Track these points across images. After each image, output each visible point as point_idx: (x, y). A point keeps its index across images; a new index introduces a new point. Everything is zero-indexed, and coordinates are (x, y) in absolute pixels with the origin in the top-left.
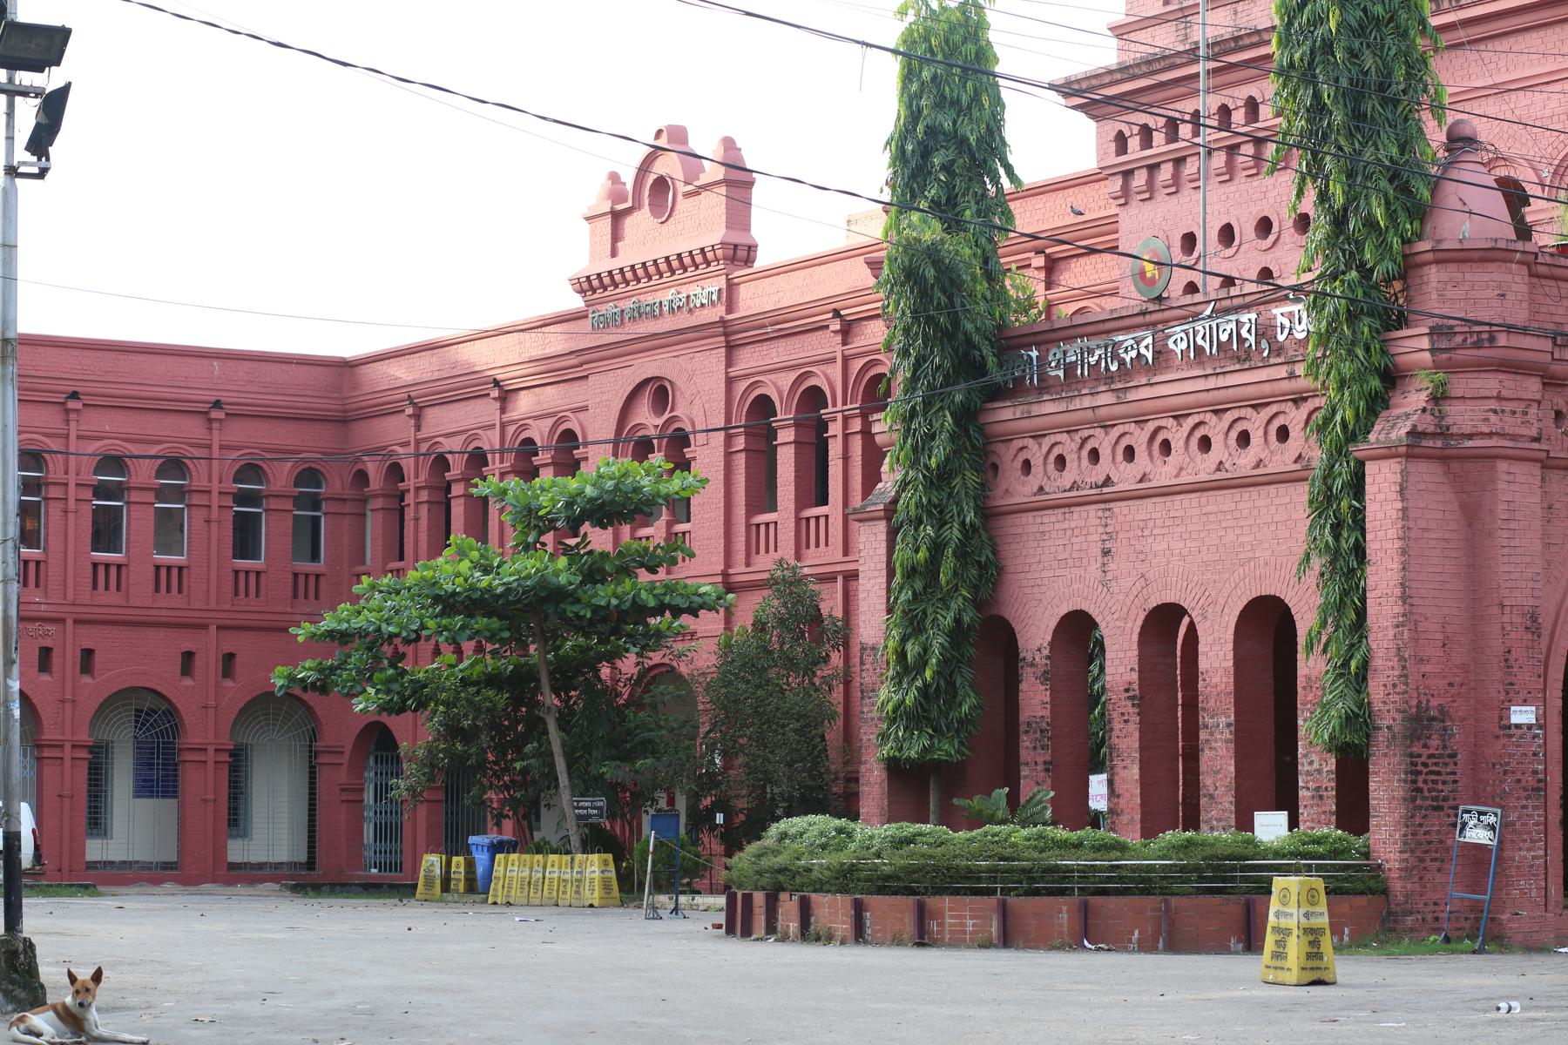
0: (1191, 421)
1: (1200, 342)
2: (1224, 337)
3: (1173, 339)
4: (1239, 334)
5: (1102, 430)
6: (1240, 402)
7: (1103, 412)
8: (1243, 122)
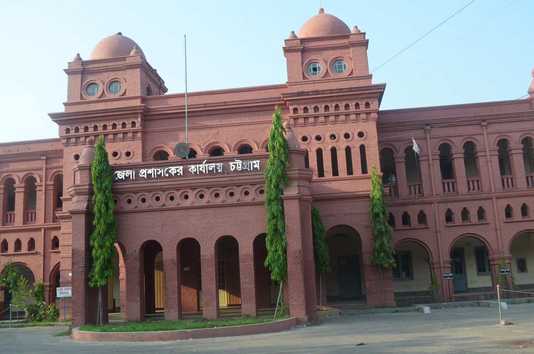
0: (197, 190)
1: (201, 169)
2: (211, 169)
4: (216, 168)
5: (162, 192)
7: (164, 187)
8: (111, 129)
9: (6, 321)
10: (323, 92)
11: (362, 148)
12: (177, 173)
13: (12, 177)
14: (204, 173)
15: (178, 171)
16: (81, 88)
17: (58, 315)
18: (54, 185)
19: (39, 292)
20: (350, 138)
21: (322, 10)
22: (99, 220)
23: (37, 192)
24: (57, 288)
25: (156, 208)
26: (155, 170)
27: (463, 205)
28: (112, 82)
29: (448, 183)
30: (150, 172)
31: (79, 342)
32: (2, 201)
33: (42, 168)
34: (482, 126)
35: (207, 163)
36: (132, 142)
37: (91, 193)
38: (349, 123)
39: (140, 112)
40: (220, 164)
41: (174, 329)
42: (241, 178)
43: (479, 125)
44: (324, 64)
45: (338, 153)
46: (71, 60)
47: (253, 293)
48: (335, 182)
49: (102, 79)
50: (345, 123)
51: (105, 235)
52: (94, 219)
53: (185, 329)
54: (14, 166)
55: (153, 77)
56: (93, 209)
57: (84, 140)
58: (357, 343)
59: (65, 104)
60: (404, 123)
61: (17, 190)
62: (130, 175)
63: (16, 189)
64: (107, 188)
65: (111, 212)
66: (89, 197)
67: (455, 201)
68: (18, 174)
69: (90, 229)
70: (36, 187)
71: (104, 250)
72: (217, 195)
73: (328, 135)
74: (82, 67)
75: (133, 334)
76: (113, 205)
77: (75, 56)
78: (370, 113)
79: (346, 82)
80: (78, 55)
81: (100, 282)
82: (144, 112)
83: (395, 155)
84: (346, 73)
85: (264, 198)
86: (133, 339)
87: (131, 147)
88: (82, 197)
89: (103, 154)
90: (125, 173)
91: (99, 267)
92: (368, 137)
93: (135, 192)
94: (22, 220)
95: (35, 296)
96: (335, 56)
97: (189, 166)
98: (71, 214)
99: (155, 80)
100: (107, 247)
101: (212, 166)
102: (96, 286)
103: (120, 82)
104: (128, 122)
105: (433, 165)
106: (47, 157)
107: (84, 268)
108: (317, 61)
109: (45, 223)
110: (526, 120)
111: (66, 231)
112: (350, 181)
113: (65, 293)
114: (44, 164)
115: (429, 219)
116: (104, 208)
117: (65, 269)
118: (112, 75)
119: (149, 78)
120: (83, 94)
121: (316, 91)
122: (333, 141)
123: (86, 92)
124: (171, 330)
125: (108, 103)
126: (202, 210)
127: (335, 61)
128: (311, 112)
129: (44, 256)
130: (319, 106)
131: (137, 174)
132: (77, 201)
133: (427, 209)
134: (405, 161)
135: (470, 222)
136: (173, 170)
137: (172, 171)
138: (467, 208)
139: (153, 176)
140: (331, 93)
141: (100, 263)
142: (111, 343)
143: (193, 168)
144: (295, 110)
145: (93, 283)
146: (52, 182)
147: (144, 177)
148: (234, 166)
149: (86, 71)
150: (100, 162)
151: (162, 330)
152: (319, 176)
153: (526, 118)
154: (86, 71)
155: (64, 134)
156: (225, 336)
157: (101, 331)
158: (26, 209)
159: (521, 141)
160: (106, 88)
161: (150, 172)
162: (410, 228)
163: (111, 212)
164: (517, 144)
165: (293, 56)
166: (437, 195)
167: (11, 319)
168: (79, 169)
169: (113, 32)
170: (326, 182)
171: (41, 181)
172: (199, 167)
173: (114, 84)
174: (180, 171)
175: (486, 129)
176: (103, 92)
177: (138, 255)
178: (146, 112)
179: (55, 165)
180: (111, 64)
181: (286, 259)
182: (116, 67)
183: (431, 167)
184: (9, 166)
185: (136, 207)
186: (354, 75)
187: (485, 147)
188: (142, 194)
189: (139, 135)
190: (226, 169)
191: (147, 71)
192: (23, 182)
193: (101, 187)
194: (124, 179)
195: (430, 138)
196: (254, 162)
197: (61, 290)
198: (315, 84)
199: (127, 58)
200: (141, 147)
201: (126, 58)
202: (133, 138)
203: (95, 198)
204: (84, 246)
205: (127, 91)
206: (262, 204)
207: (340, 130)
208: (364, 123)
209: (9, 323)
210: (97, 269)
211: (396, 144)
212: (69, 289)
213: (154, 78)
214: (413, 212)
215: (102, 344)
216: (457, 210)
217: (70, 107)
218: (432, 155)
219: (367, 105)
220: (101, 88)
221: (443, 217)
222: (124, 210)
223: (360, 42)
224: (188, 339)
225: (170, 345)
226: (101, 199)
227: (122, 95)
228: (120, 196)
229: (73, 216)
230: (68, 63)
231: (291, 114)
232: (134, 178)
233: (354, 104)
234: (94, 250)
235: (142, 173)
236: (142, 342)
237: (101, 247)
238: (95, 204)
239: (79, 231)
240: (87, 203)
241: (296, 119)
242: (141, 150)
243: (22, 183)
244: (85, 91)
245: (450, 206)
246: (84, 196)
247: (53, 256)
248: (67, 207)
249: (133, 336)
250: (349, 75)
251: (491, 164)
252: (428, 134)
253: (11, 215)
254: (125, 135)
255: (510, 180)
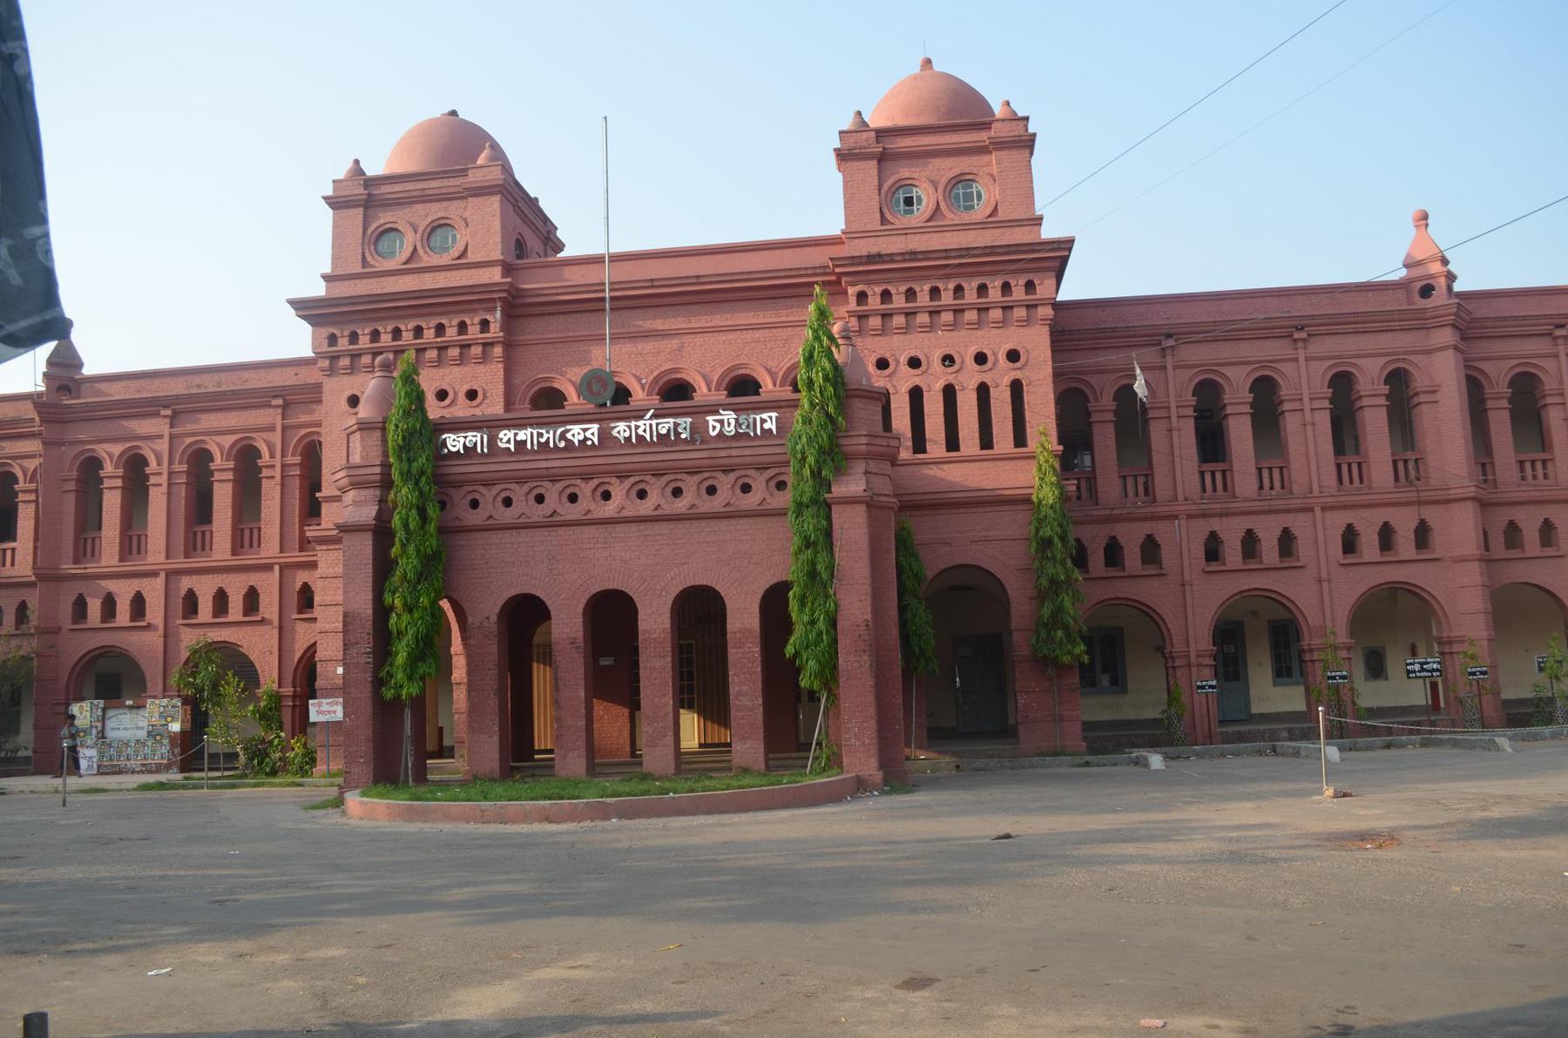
0: (632, 480)
1: (640, 432)
2: (664, 431)
3: (617, 430)
4: (675, 429)
5: (550, 483)
6: (677, 470)
7: (555, 471)
8: (432, 336)
9: (196, 775)
10: (927, 254)
11: (1016, 388)
12: (586, 439)
13: (204, 446)
14: (649, 439)
15: (588, 434)
16: (363, 240)
17: (313, 762)
18: (301, 465)
19: (270, 709)
20: (989, 365)
21: (928, 63)
22: (404, 546)
23: (264, 482)
24: (311, 702)
25: (535, 519)
26: (535, 432)
27: (1245, 523)
28: (437, 226)
29: (1213, 474)
30: (522, 436)
31: (360, 822)
32: (183, 501)
33: (275, 427)
34: (1295, 341)
35: (655, 416)
36: (481, 367)
37: (386, 483)
38: (987, 329)
39: (499, 298)
40: (770, 414)
41: (577, 798)
42: (734, 452)
43: (1289, 339)
44: (931, 190)
45: (960, 397)
46: (341, 174)
47: (760, 718)
48: (952, 466)
49: (412, 220)
50: (976, 329)
51: (419, 582)
52: (393, 544)
53: (602, 797)
54: (209, 421)
55: (530, 216)
56: (390, 522)
57: (370, 361)
58: (997, 834)
59: (326, 278)
60: (1114, 330)
61: (217, 476)
62: (475, 444)
63: (216, 473)
64: (422, 473)
65: (432, 528)
66: (381, 491)
67: (1227, 515)
68: (218, 439)
69: (383, 568)
70: (260, 470)
71: (416, 616)
72: (677, 492)
73: (936, 356)
74: (366, 192)
75: (483, 808)
76: (437, 512)
77: (349, 165)
78: (1036, 306)
79: (981, 231)
80: (357, 162)
81: (408, 689)
82: (509, 298)
83: (1092, 406)
84: (981, 211)
85: (785, 499)
86: (482, 817)
87: (479, 379)
88: (365, 492)
89: (415, 394)
90: (465, 437)
91: (405, 654)
92: (1029, 363)
93: (488, 484)
94: (229, 546)
95: (261, 719)
96: (957, 171)
97: (612, 425)
98: (341, 531)
99: (535, 221)
100: (422, 608)
101: (666, 425)
102: (398, 697)
103: (454, 227)
104: (472, 321)
105: (1179, 430)
106: (285, 400)
107: (371, 656)
108: (913, 182)
109: (281, 552)
110: (1397, 328)
111: (330, 572)
112: (986, 464)
113: (329, 712)
114: (280, 417)
115: (1168, 556)
116: (415, 518)
117: (329, 659)
118: (435, 211)
119: (522, 218)
120: (367, 254)
121: (911, 253)
122: (950, 370)
123: (375, 249)
124: (569, 799)
125: (426, 275)
126: (643, 526)
127: (957, 183)
128: (899, 301)
129: (281, 628)
130: (917, 289)
131: (493, 440)
132: (355, 503)
133: (1161, 531)
134: (1252, 411)
135: (1261, 562)
136: (576, 432)
137: (573, 435)
138: (1255, 531)
139: (529, 446)
140: (946, 258)
141: (408, 646)
142: (434, 825)
143: (621, 429)
144: (862, 297)
145: (392, 691)
146: (297, 460)
147: (509, 449)
148: (718, 426)
149: (374, 201)
150: (407, 413)
151: (550, 799)
152: (915, 452)
153: (1397, 323)
154: (374, 201)
155: (325, 348)
156: (693, 814)
157: (408, 800)
158: (238, 519)
159: (1383, 377)
160: (422, 240)
161: (522, 436)
162: (1122, 574)
163: (432, 528)
164: (1376, 383)
165: (859, 169)
166: (1186, 499)
167: (206, 769)
168: (359, 429)
169: (438, 111)
170: (931, 466)
171: (272, 456)
172: (637, 427)
173: (439, 232)
174: (593, 434)
175: (1305, 348)
176: (415, 248)
177: (494, 628)
178: (513, 297)
179: (304, 418)
180: (433, 184)
181: (835, 641)
182: (444, 191)
183: (1175, 433)
184: (198, 421)
185: (491, 517)
186: (1001, 216)
187: (1301, 390)
188: (502, 486)
189: (498, 350)
190: (698, 430)
191: (517, 202)
192: (232, 459)
193: (409, 471)
194: (462, 452)
195: (1175, 368)
196: (765, 416)
197: (320, 705)
198: (909, 236)
199: (470, 172)
200: (502, 380)
201: (467, 170)
202: (484, 359)
203: (395, 496)
204: (371, 606)
205: (469, 247)
206: (781, 513)
207: (965, 344)
208: (1021, 329)
209: (203, 779)
210: (401, 658)
211: (1092, 379)
212: (337, 703)
213: (532, 219)
214: (1131, 538)
215: (413, 827)
216: (1231, 534)
217: (338, 283)
218: (1178, 407)
219: (1030, 286)
220: (409, 240)
221: (1199, 552)
222: (461, 524)
223: (1017, 138)
224: (610, 820)
225: (568, 833)
226: (407, 498)
227: (459, 258)
228: (452, 491)
229: (346, 537)
230: (334, 181)
231: (852, 304)
232: (486, 450)
233: (998, 283)
234: (394, 615)
235: (505, 440)
236: (502, 826)
237: (409, 609)
238: (394, 509)
239: (359, 572)
240: (377, 507)
241: (862, 317)
242: (501, 387)
243: (228, 460)
244: (372, 248)
245: (1216, 525)
246: (371, 491)
247: (301, 628)
248: (331, 516)
249: (483, 811)
250: (989, 216)
251: (1314, 429)
252: (1169, 358)
253: (203, 533)
254: (465, 351)
255: (1355, 468)
